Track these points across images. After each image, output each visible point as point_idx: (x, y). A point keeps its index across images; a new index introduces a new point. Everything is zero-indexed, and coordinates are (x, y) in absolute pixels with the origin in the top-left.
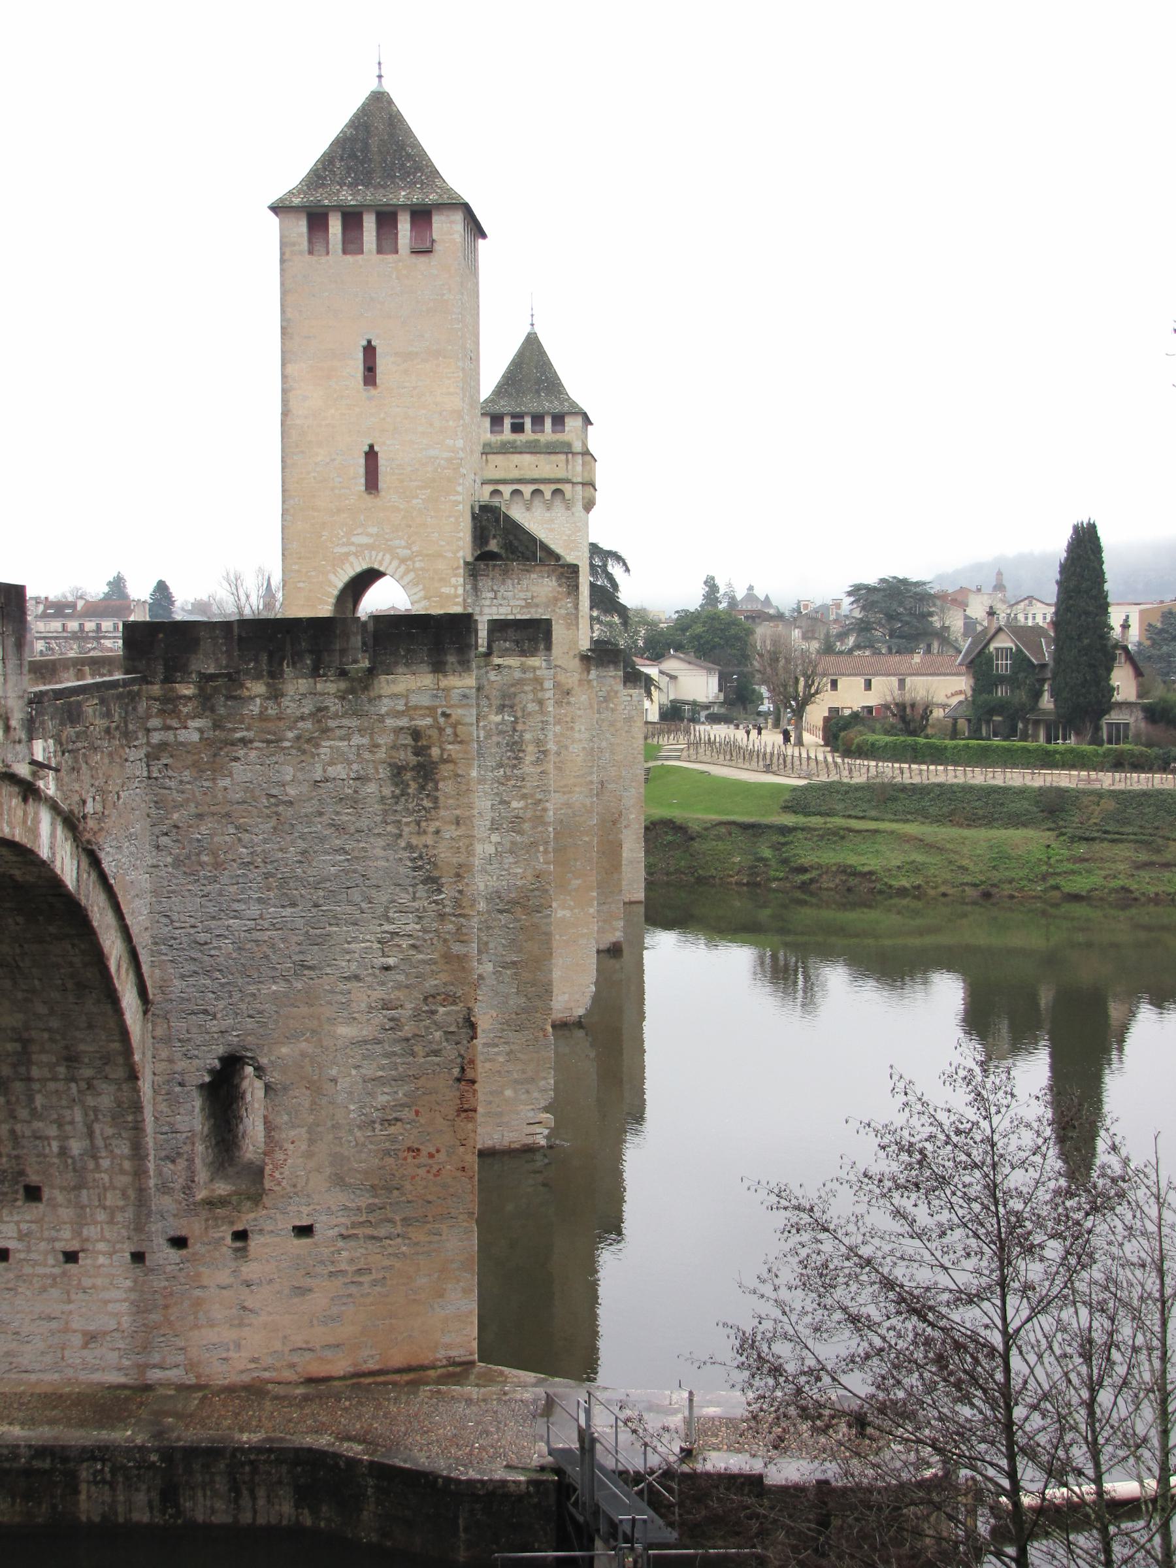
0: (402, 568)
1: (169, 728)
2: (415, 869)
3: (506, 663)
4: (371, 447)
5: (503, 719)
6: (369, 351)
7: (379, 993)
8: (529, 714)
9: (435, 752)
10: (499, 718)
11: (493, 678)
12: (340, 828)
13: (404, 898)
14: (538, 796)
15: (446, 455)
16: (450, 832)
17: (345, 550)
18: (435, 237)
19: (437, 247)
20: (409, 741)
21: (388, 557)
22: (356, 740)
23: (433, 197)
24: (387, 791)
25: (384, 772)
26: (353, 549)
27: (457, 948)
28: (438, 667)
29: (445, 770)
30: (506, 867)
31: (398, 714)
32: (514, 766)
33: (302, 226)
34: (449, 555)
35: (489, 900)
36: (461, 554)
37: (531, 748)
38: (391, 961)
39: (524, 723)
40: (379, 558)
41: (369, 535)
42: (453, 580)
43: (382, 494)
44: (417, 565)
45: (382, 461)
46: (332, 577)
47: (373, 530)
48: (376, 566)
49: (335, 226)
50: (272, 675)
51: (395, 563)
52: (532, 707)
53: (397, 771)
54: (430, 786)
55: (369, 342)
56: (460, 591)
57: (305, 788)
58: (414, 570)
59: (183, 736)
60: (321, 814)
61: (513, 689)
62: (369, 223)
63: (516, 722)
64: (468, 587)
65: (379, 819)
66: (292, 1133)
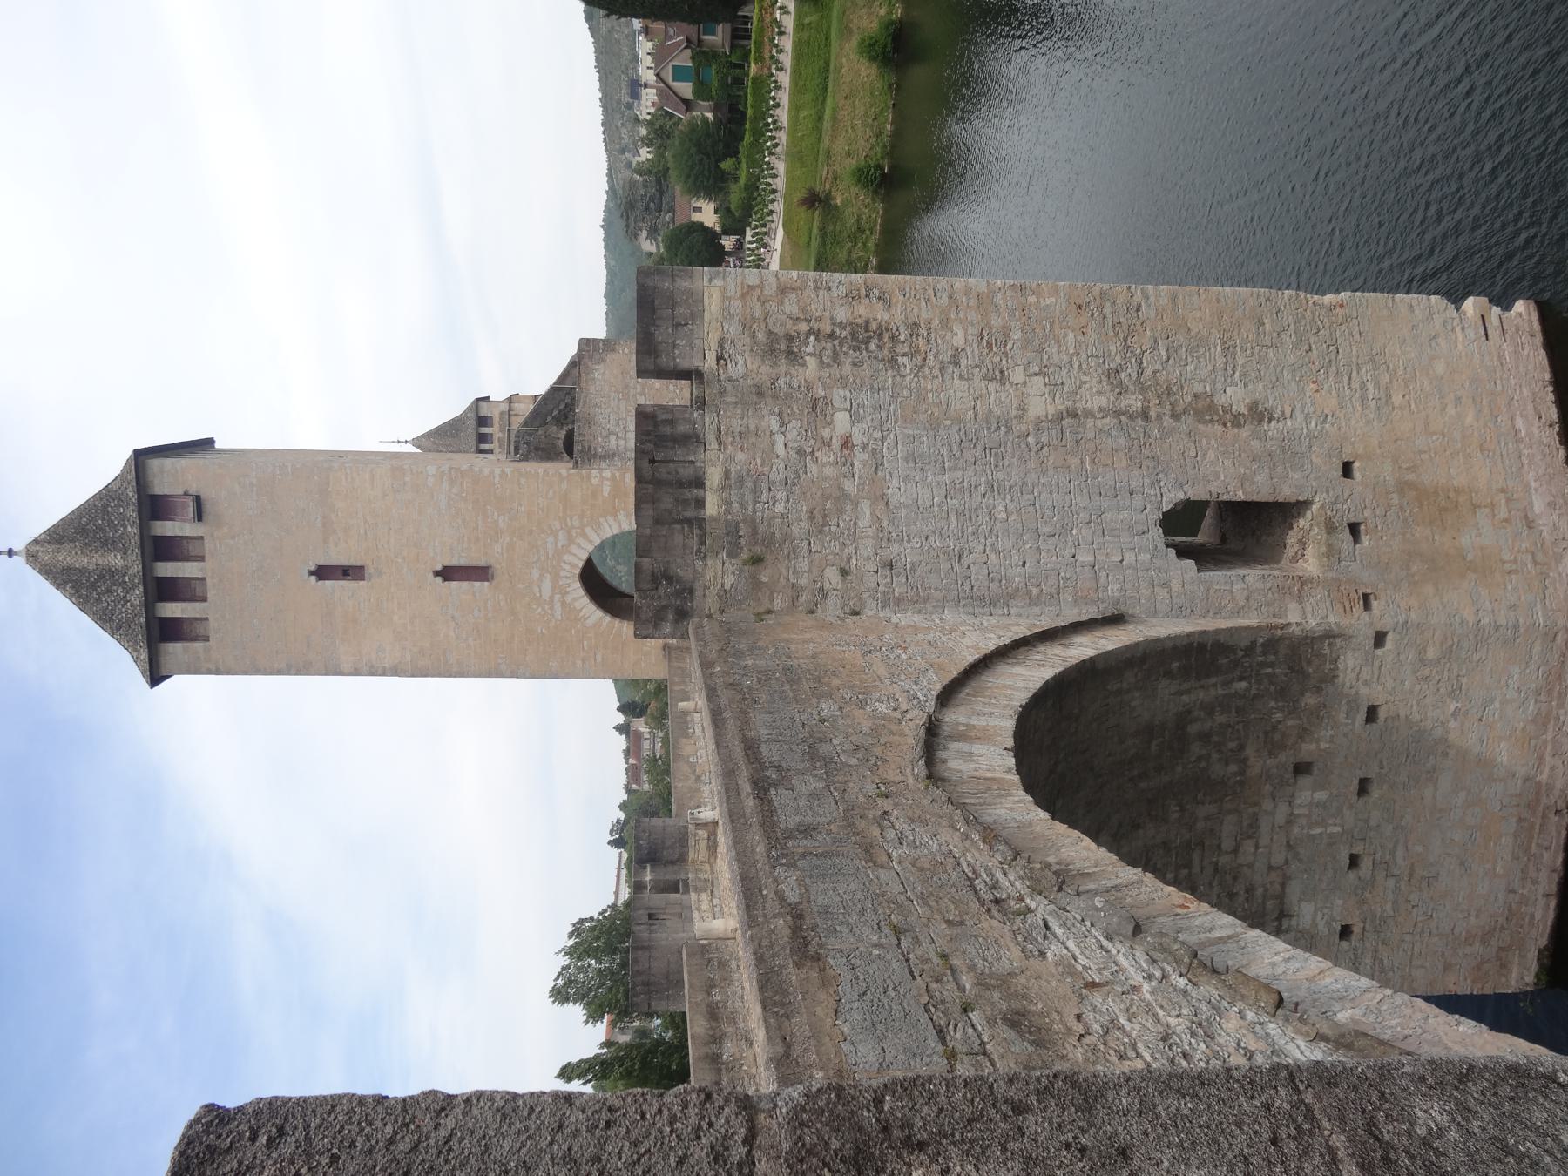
0: (580, 540)
3: (714, 346)
4: (437, 573)
5: (813, 354)
6: (322, 573)
8: (804, 310)
10: (811, 362)
11: (741, 368)
14: (944, 300)
15: (445, 485)
17: (558, 606)
18: (181, 492)
19: (193, 491)
21: (566, 557)
23: (131, 493)
26: (557, 597)
30: (1066, 359)
32: (893, 338)
33: (174, 649)
34: (564, 486)
35: (1122, 390)
36: (564, 472)
37: (862, 310)
39: (819, 319)
40: (567, 567)
41: (542, 576)
42: (595, 481)
43: (492, 562)
44: (576, 523)
45: (454, 561)
46: (590, 622)
48: (578, 571)
49: (172, 610)
51: (574, 549)
52: (791, 306)
55: (312, 573)
56: (607, 474)
61: (761, 336)
62: (166, 569)
63: (818, 334)
64: (603, 465)
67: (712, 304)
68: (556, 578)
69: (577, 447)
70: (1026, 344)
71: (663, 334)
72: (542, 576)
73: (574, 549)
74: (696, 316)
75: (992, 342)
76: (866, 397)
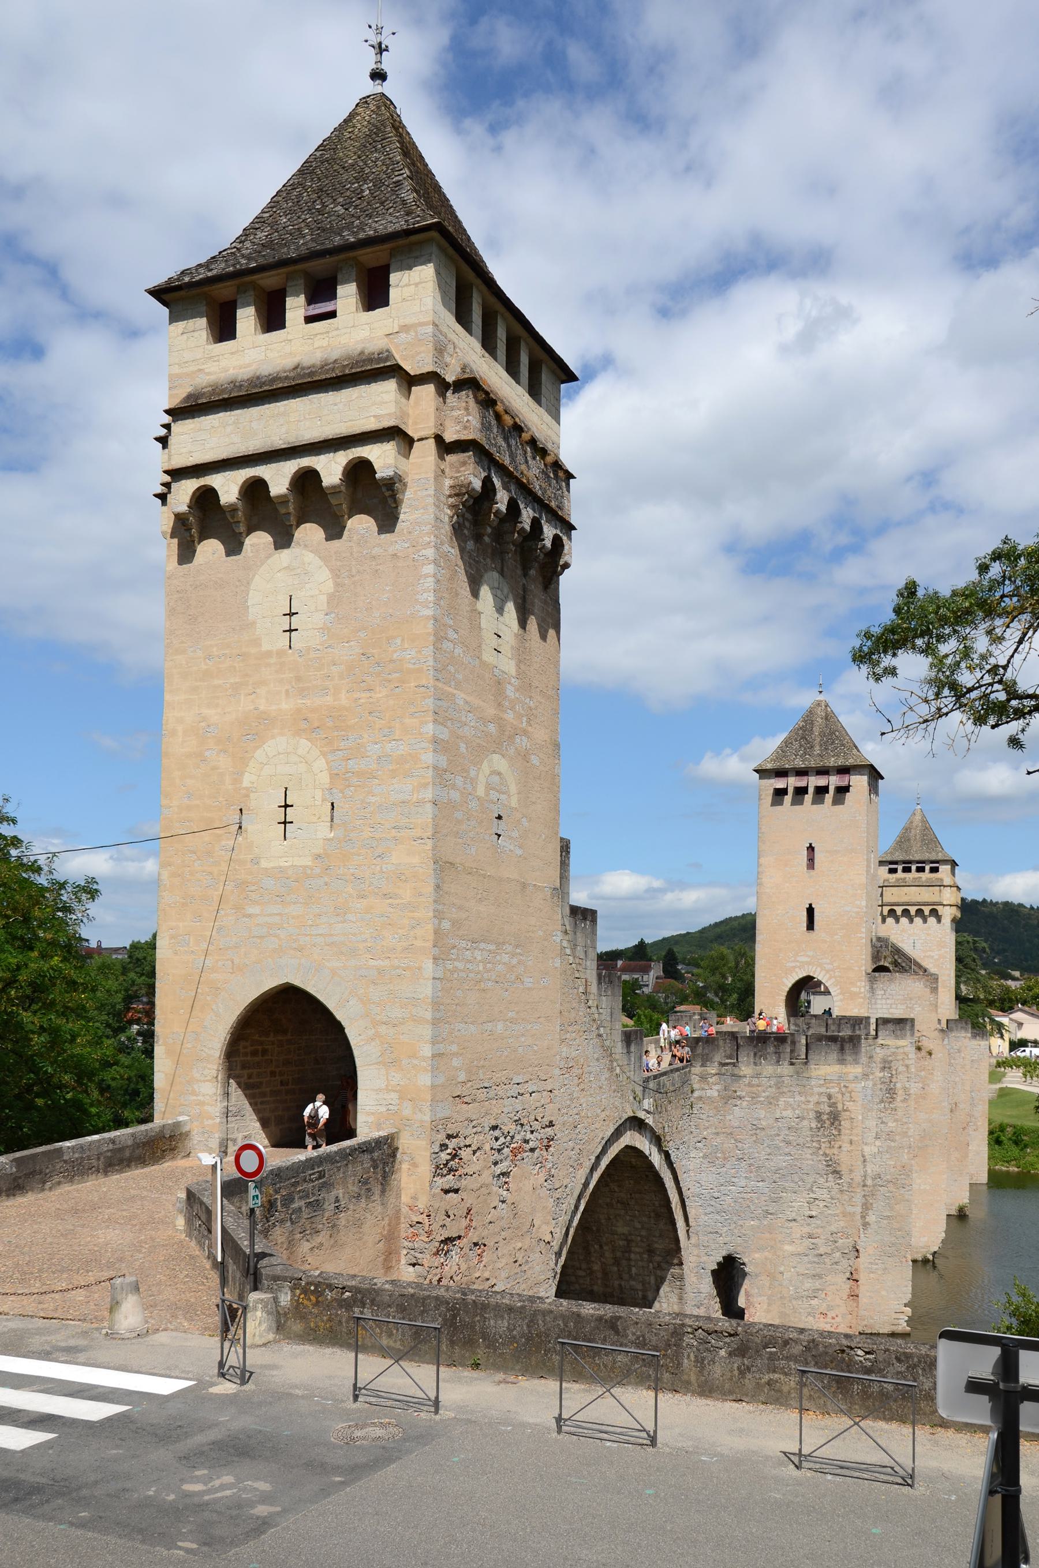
0: (828, 976)
1: (703, 1089)
2: (828, 1166)
4: (810, 905)
6: (811, 848)
7: (806, 1230)
9: (840, 1107)
10: (881, 1075)
12: (788, 1143)
13: (822, 1180)
14: (904, 1120)
16: (846, 1146)
17: (793, 964)
20: (826, 1099)
21: (819, 969)
22: (798, 1098)
24: (813, 1125)
25: (812, 1115)
27: (850, 1209)
28: (842, 1061)
29: (844, 1115)
31: (821, 1086)
35: (874, 1179)
36: (863, 968)
37: (900, 1092)
38: (814, 1213)
41: (808, 956)
42: (859, 984)
46: (785, 980)
47: (810, 953)
50: (755, 1064)
51: (823, 972)
52: (901, 1069)
53: (819, 1115)
54: (837, 1123)
57: (771, 1121)
58: (835, 977)
59: (709, 1093)
60: (779, 1135)
65: (808, 1139)
66: (760, 1299)
67: (901, 1043)
68: (809, 963)
69: (877, 974)
70: (889, 1147)
71: (890, 1026)
72: (808, 956)
73: (823, 972)
74: (897, 1037)
75: (890, 1136)
76: (869, 1092)
